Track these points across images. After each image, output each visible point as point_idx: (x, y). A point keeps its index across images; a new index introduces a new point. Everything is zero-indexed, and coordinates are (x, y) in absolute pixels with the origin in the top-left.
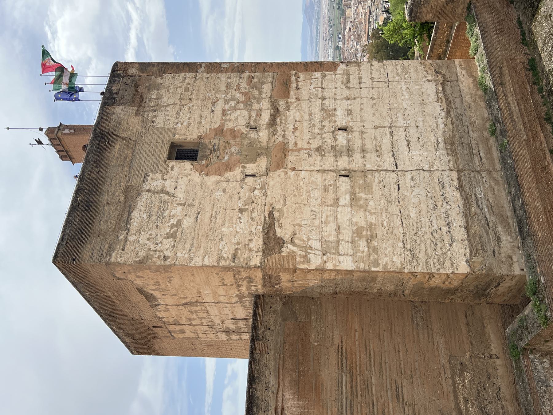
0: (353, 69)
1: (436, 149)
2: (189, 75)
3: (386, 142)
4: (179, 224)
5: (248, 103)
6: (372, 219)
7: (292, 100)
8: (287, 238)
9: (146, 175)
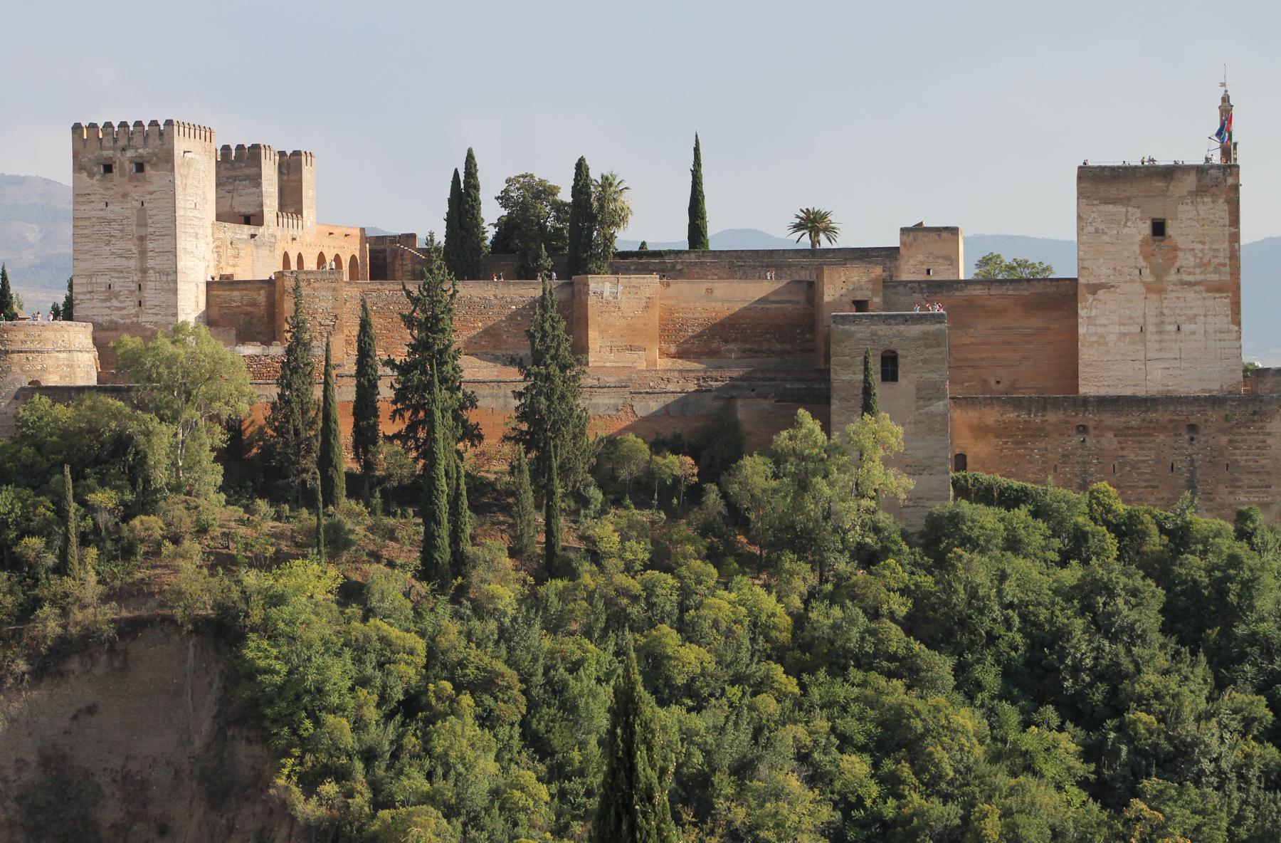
0: (1234, 335)
1: (1163, 385)
2: (1227, 222)
5: (1202, 265)
6: (1111, 344)
7: (1204, 294)
8: (1096, 296)
9: (1138, 207)
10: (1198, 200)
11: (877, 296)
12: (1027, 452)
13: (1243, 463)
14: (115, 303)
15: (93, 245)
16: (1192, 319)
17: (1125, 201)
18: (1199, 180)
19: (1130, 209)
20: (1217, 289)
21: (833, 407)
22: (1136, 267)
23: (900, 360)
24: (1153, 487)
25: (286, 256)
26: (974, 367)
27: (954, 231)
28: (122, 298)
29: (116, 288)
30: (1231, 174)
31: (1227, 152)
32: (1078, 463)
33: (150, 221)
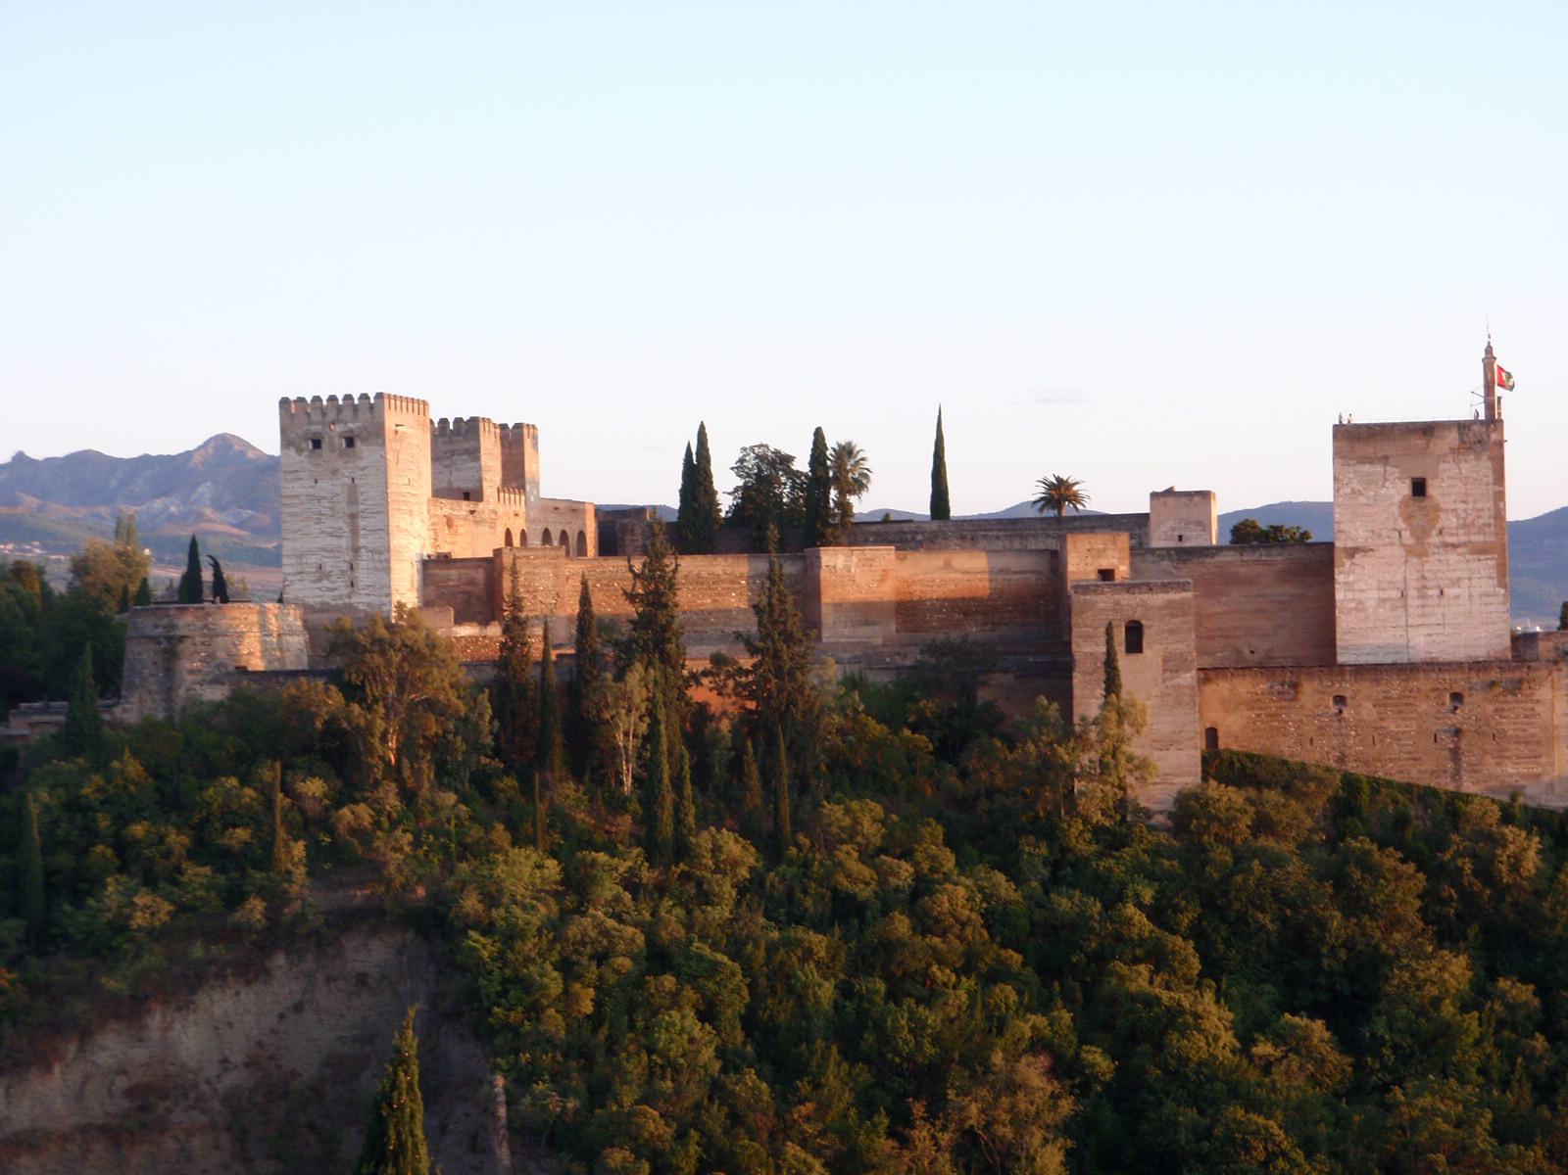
2: (1491, 480)
3: (1433, 620)
4: (1361, 494)
6: (1371, 610)
7: (1468, 557)
10: (1461, 457)
11: (1123, 564)
12: (1281, 725)
13: (1511, 732)
14: (326, 583)
15: (302, 524)
16: (1456, 583)
17: (1385, 460)
18: (1461, 436)
19: (1388, 468)
20: (1481, 550)
21: (1076, 681)
22: (1395, 529)
23: (1146, 631)
24: (1414, 759)
25: (508, 533)
26: (1227, 637)
27: (1205, 496)
28: (333, 578)
29: (328, 568)
30: (1495, 430)
31: (1491, 405)
32: (1335, 735)
33: (361, 498)
